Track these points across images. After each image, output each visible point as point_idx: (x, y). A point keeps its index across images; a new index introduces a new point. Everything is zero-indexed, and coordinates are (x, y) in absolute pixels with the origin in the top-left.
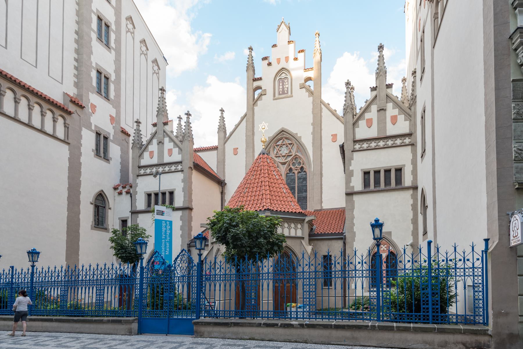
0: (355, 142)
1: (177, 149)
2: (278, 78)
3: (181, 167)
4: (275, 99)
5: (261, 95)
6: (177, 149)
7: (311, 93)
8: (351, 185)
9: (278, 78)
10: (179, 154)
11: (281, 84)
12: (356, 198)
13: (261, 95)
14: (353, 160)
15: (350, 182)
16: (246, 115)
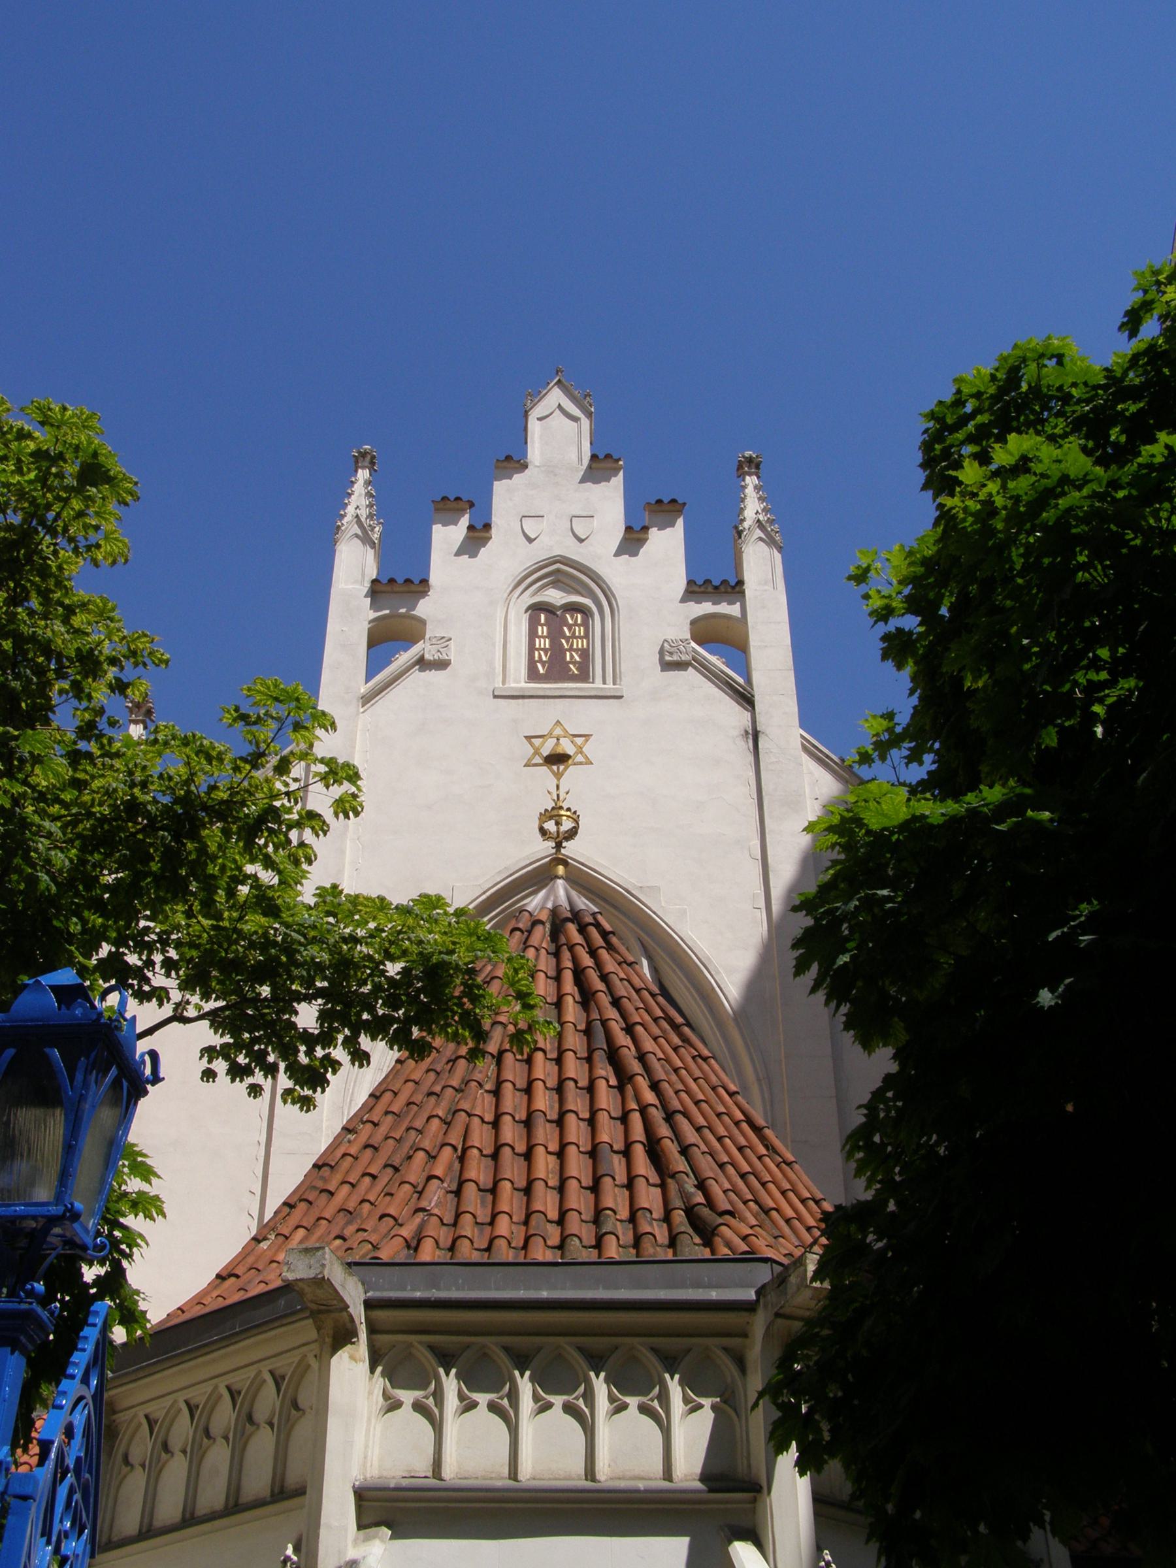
11: (542, 630)
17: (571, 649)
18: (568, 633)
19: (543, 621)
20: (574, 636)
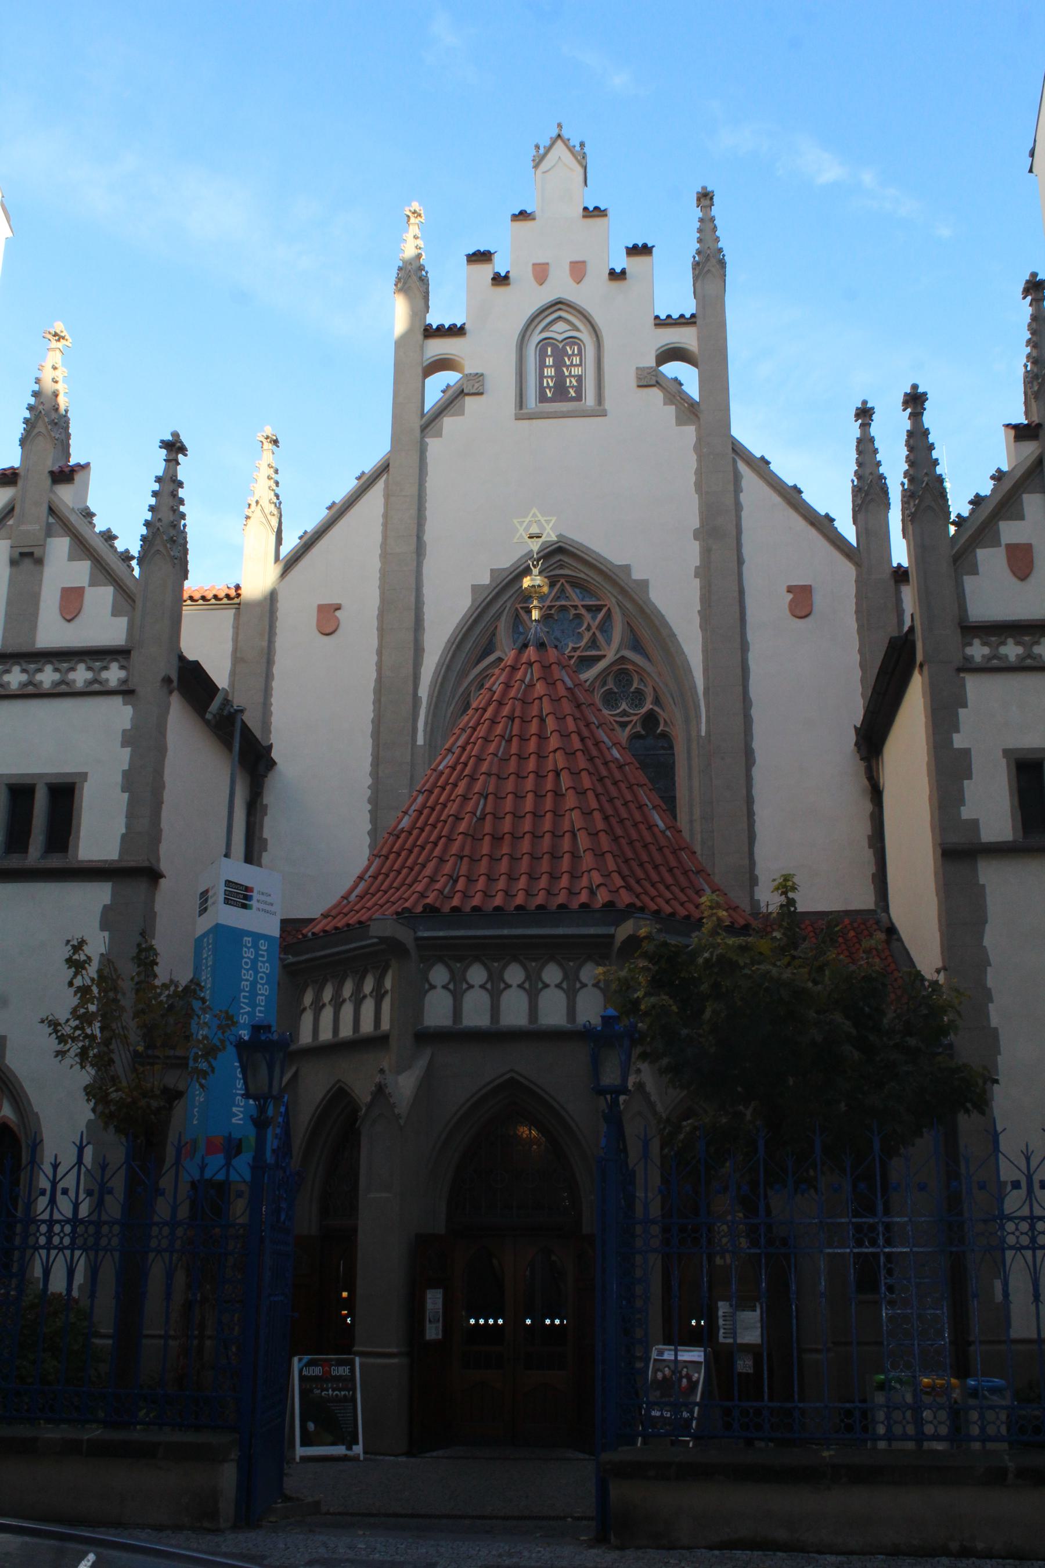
0: (972, 630)
1: (110, 590)
2: (536, 338)
3: (122, 674)
4: (522, 412)
5: (461, 393)
6: (107, 593)
7: (689, 411)
8: (967, 813)
9: (536, 338)
10: (116, 613)
11: (549, 361)
12: (991, 875)
13: (461, 393)
14: (965, 705)
15: (961, 801)
16: (384, 468)
17: (570, 376)
18: (568, 363)
19: (549, 353)
20: (572, 365)
